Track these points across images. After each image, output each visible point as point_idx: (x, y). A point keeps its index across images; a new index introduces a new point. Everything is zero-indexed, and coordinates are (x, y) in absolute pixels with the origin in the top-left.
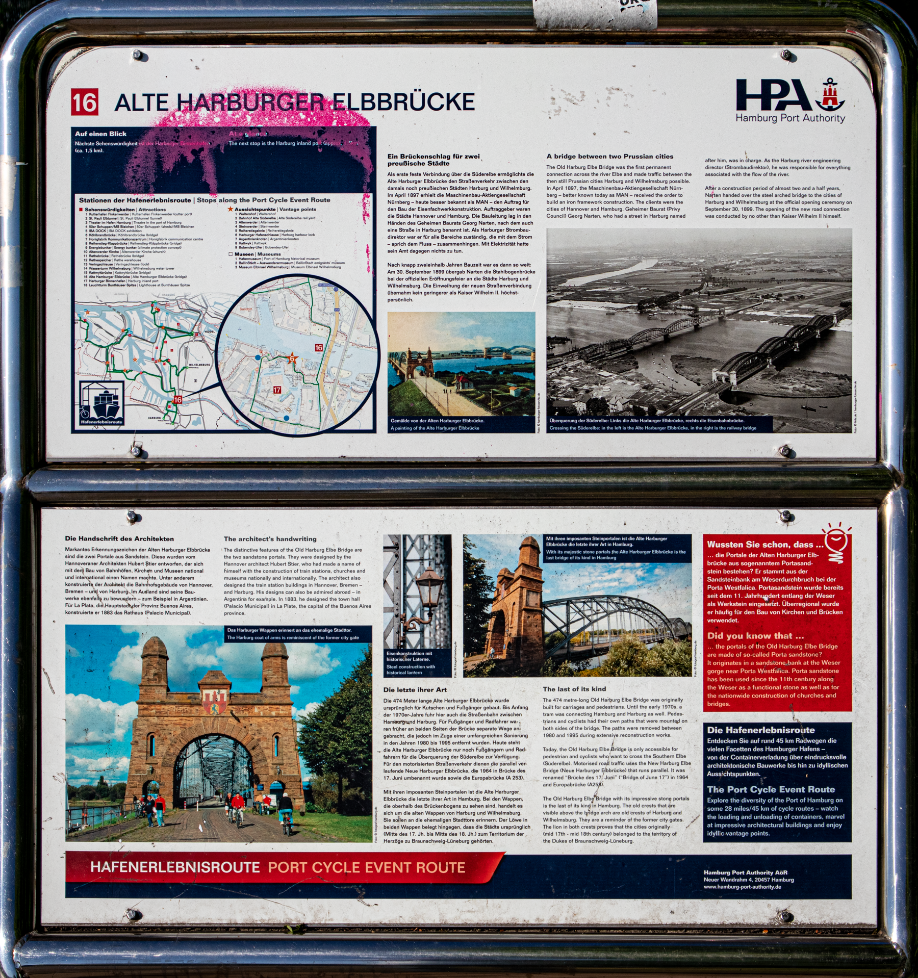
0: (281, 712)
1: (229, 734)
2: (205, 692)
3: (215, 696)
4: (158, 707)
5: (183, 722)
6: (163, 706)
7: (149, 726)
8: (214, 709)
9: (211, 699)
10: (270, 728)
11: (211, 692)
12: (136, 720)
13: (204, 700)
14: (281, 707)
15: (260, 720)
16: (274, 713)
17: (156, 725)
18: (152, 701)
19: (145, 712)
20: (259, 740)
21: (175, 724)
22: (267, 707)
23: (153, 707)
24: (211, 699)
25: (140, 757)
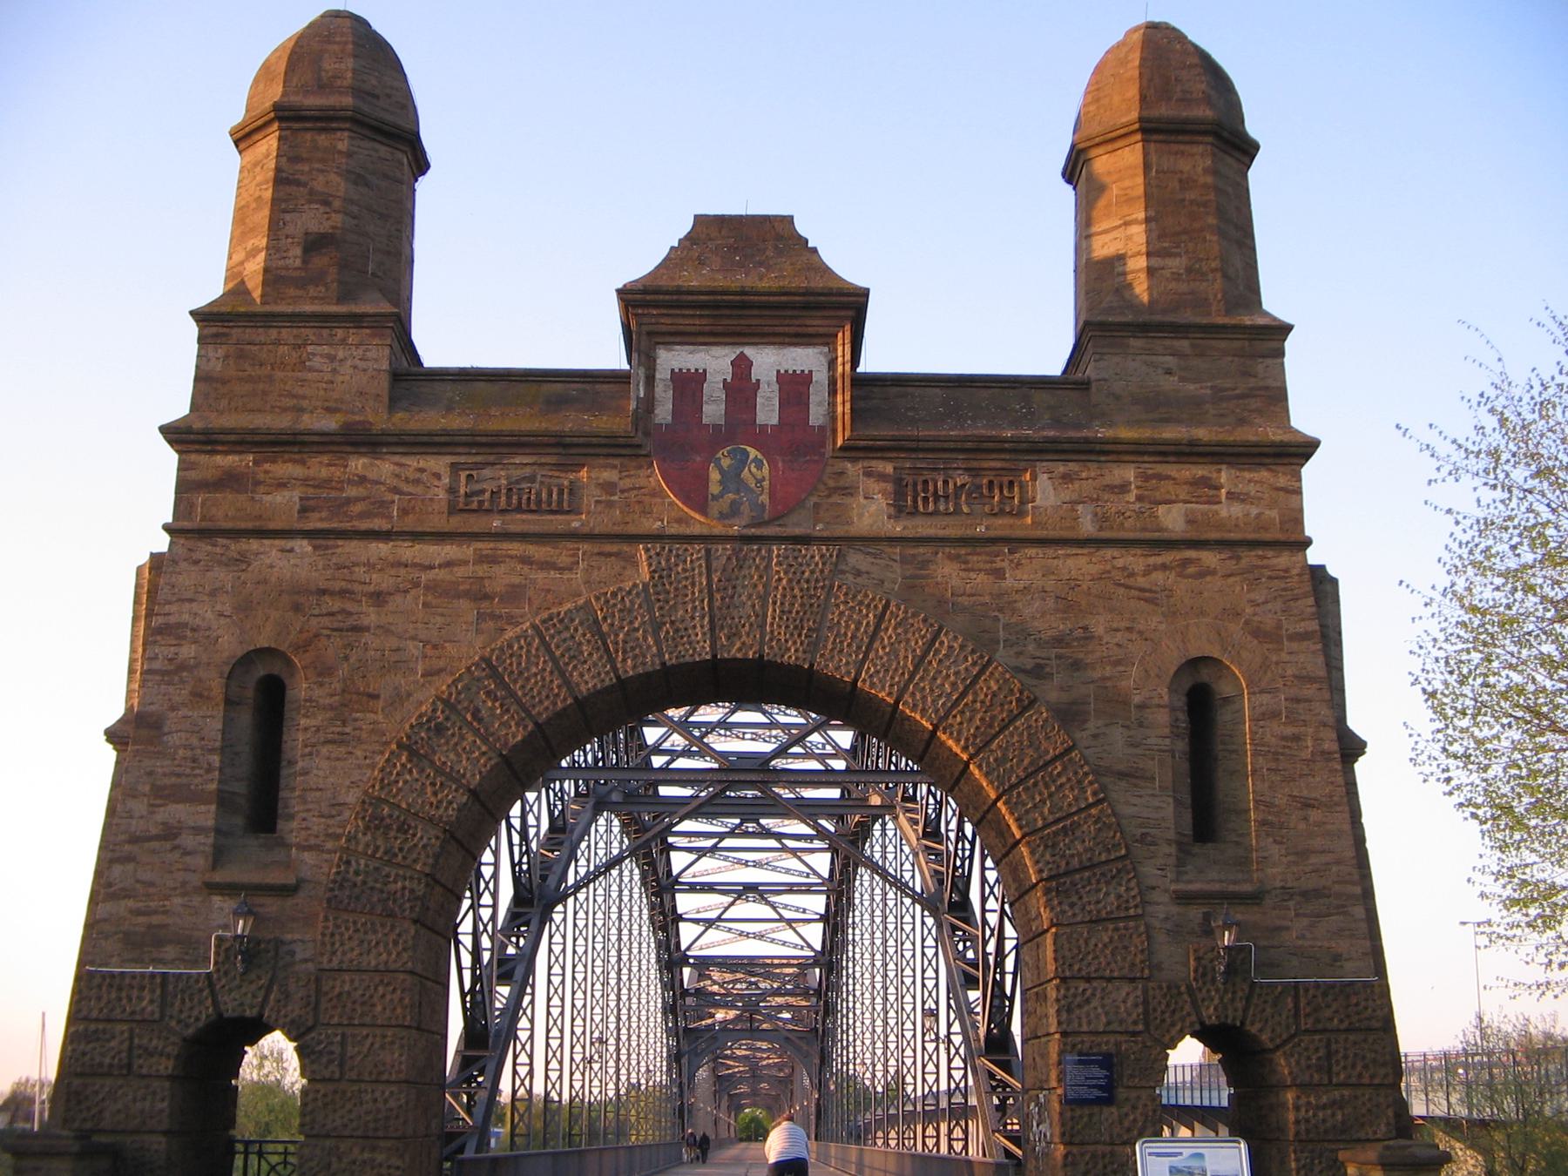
0: (1228, 511)
1: (837, 665)
2: (673, 359)
3: (741, 387)
4: (319, 467)
5: (502, 577)
6: (358, 464)
7: (245, 608)
8: (732, 478)
9: (713, 410)
10: (1153, 622)
11: (715, 362)
12: (156, 559)
13: (664, 412)
14: (1225, 476)
15: (1079, 565)
16: (1173, 519)
17: (298, 597)
18: (282, 422)
19: (226, 508)
20: (1069, 715)
21: (449, 592)
22: (1129, 473)
23: (284, 469)
24: (713, 410)
25: (170, 833)
